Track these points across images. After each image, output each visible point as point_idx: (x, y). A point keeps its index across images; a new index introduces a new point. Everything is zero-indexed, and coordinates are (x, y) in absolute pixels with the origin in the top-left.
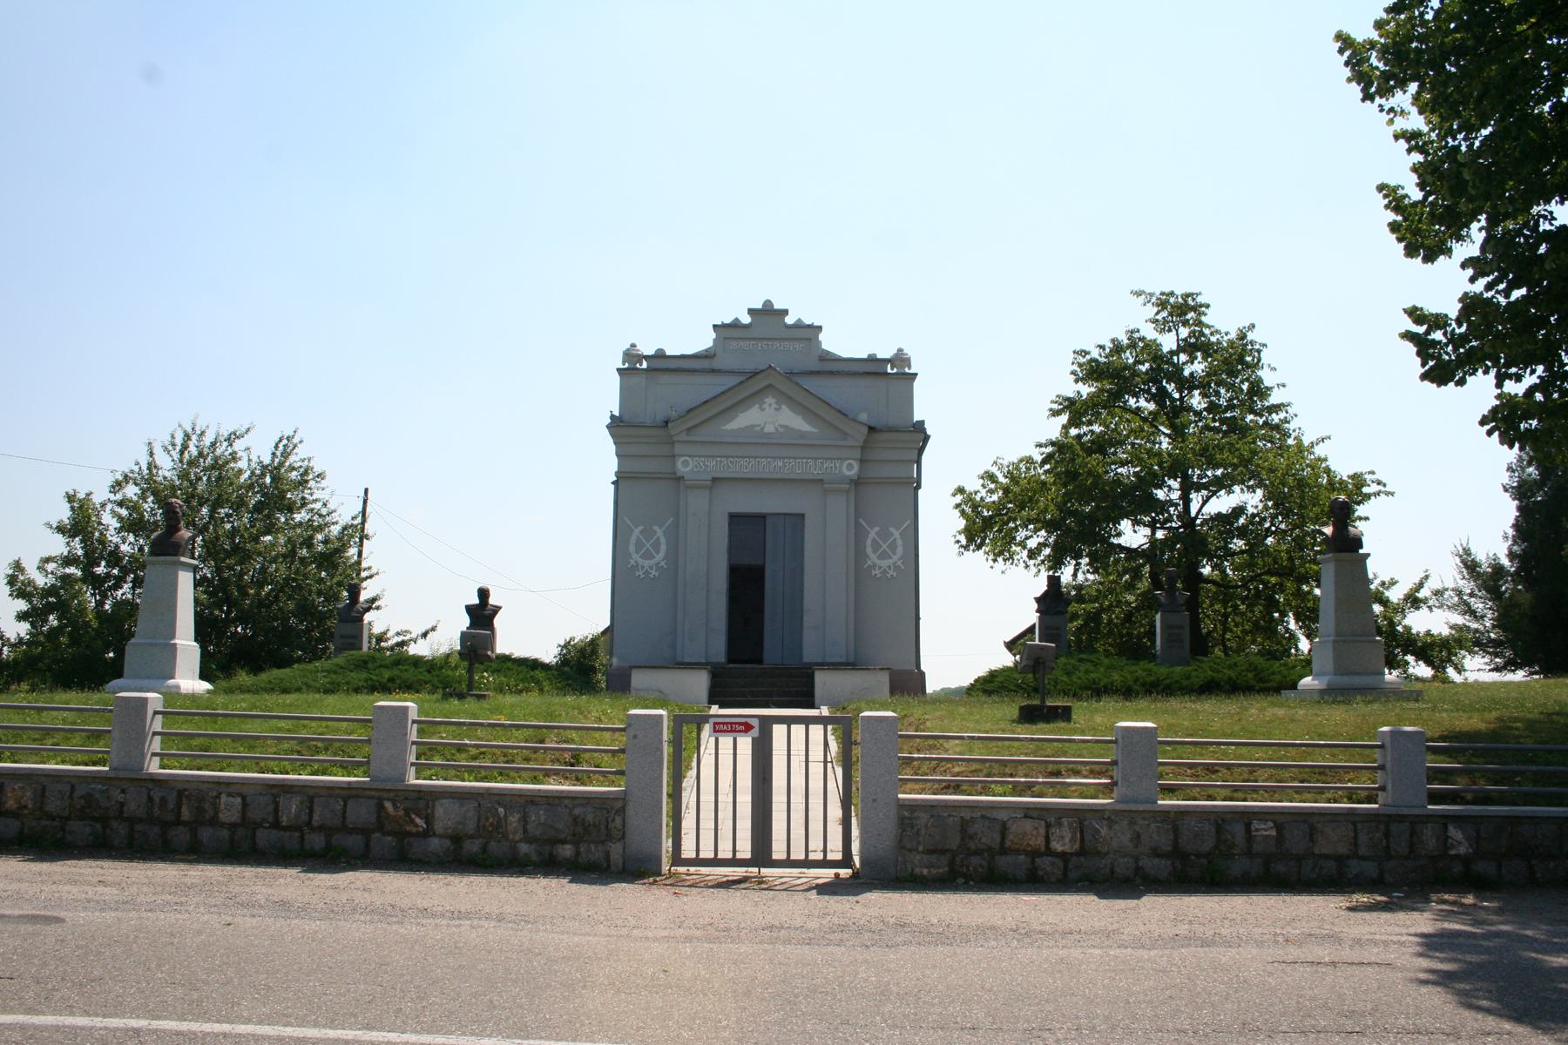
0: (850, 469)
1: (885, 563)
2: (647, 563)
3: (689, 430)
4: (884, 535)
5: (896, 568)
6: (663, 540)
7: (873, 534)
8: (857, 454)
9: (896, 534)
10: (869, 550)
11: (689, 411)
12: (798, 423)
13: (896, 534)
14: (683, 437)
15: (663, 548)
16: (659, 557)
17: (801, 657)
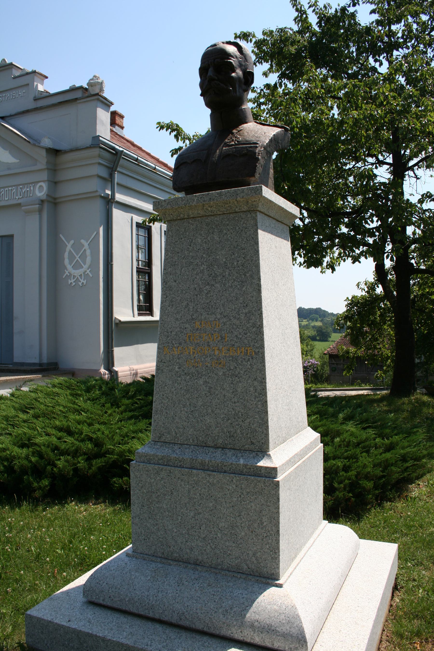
1: (77, 273)
4: (78, 247)
5: (86, 275)
7: (69, 247)
8: (45, 176)
9: (86, 244)
10: (67, 261)
13: (86, 244)
17: (13, 360)
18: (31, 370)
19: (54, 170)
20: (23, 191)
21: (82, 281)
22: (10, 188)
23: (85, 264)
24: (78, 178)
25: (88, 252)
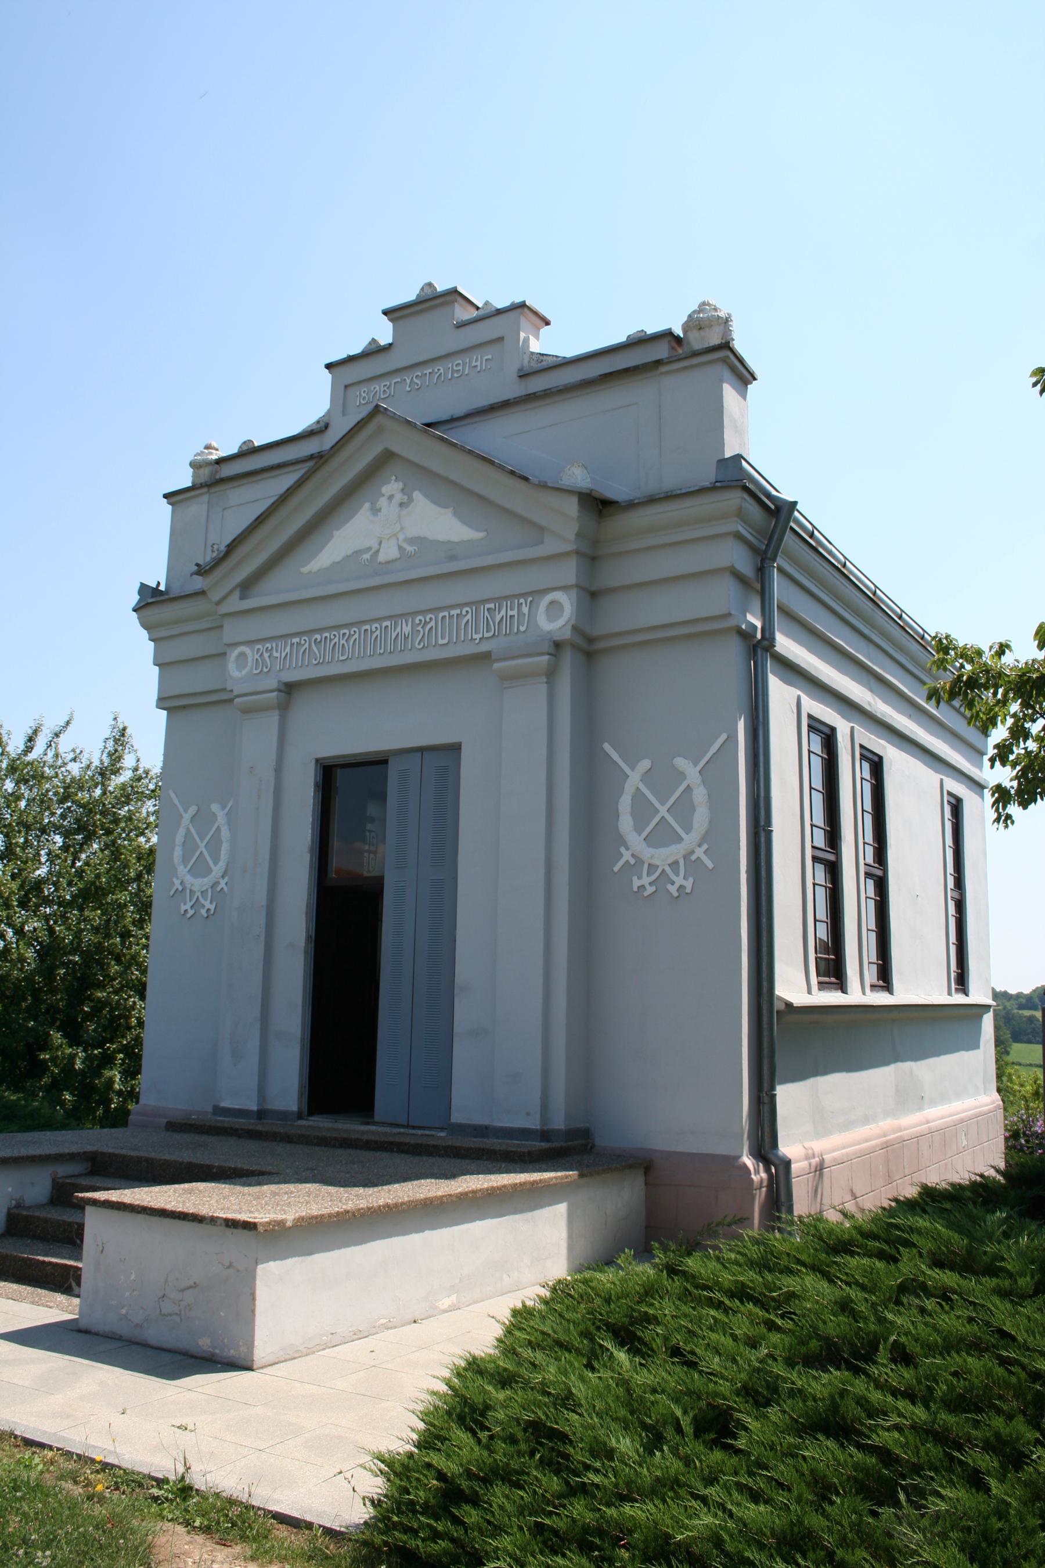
1: (662, 856)
4: (663, 778)
5: (692, 865)
7: (634, 779)
8: (569, 572)
9: (692, 773)
10: (626, 823)
13: (692, 773)
14: (235, 604)
18: (530, 1153)
19: (592, 556)
20: (498, 618)
21: (679, 881)
23: (688, 829)
25: (700, 795)
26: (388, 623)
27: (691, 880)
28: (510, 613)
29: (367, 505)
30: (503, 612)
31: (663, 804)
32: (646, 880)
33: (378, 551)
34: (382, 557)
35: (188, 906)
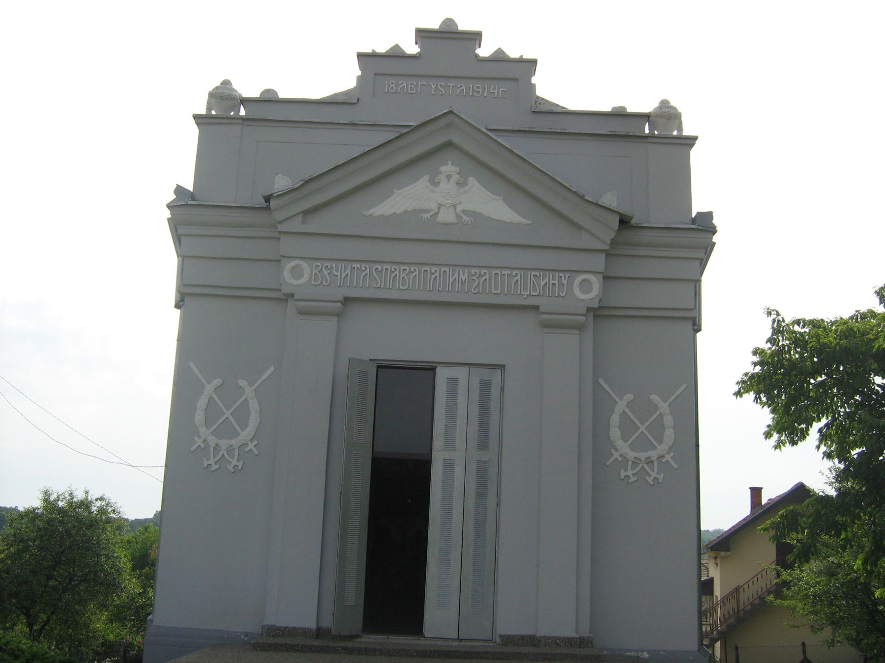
0: (587, 291)
2: (224, 444)
3: (306, 213)
6: (254, 405)
7: (621, 406)
10: (615, 433)
11: (307, 182)
12: (496, 208)
15: (254, 419)
16: (245, 435)
19: (612, 252)
20: (542, 283)
22: (506, 272)
24: (624, 278)
26: (447, 269)
27: (662, 475)
28: (552, 282)
29: (426, 177)
30: (547, 280)
31: (642, 423)
32: (630, 473)
33: (437, 213)
34: (440, 218)
35: (212, 461)
